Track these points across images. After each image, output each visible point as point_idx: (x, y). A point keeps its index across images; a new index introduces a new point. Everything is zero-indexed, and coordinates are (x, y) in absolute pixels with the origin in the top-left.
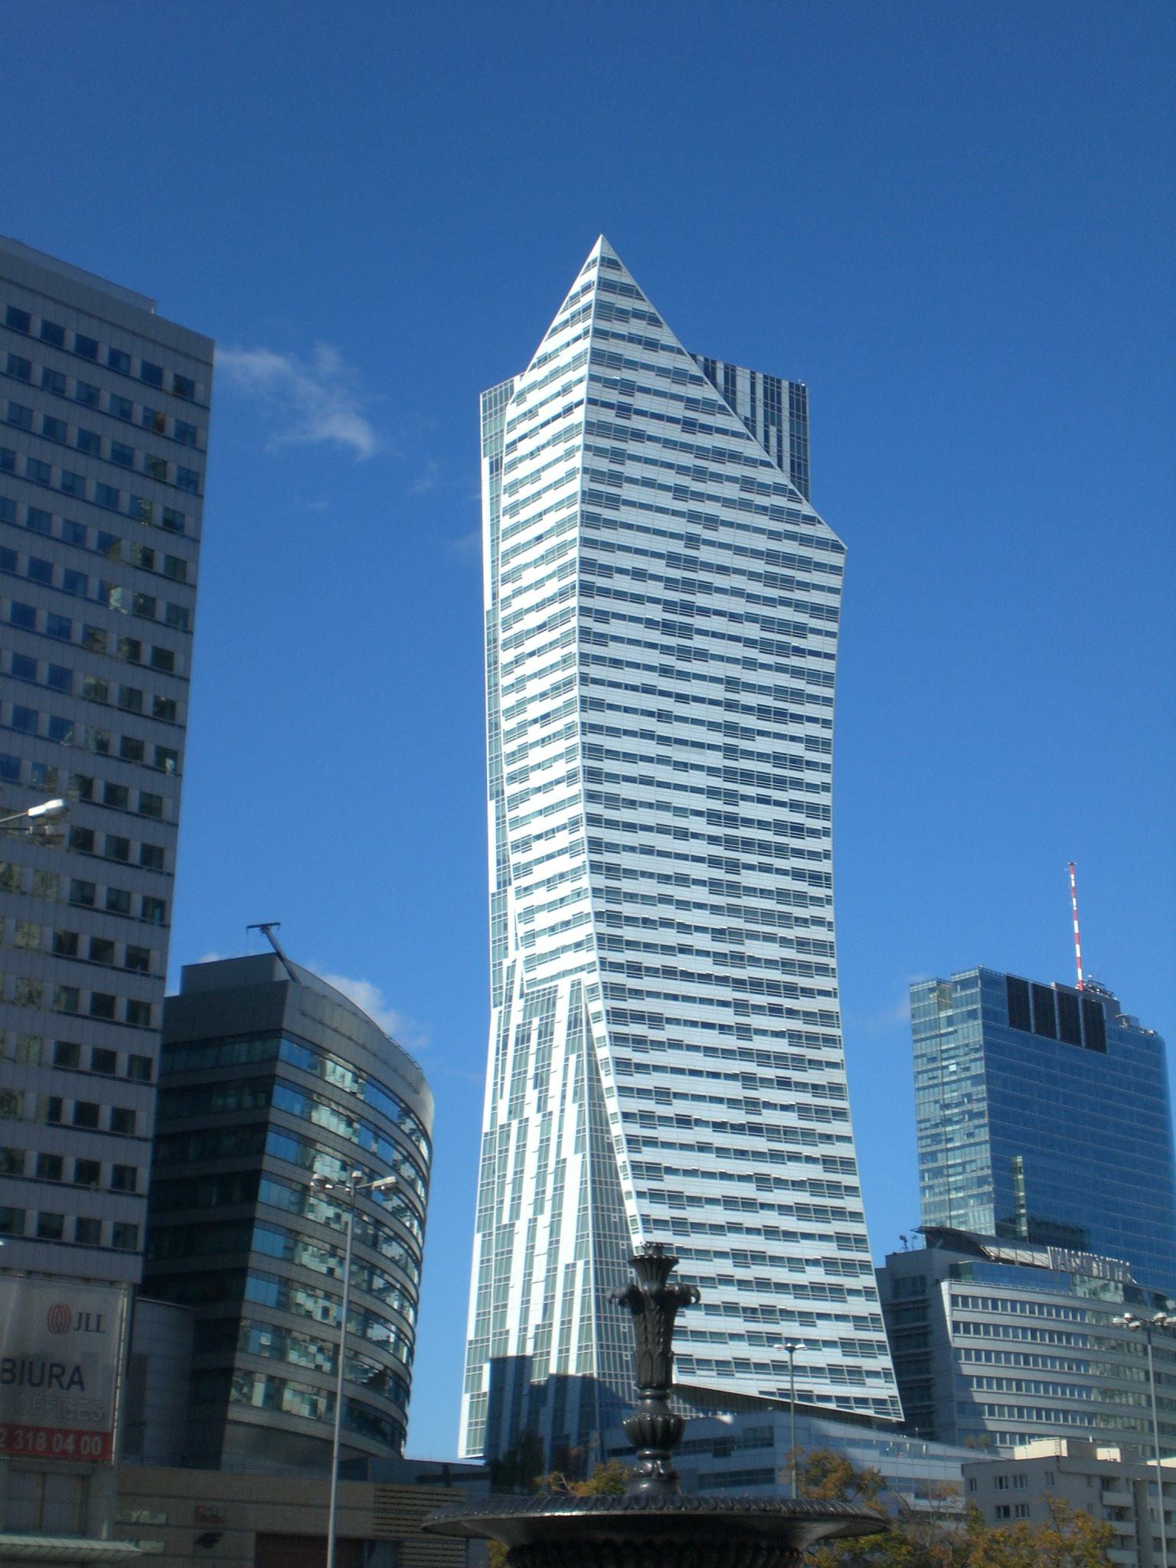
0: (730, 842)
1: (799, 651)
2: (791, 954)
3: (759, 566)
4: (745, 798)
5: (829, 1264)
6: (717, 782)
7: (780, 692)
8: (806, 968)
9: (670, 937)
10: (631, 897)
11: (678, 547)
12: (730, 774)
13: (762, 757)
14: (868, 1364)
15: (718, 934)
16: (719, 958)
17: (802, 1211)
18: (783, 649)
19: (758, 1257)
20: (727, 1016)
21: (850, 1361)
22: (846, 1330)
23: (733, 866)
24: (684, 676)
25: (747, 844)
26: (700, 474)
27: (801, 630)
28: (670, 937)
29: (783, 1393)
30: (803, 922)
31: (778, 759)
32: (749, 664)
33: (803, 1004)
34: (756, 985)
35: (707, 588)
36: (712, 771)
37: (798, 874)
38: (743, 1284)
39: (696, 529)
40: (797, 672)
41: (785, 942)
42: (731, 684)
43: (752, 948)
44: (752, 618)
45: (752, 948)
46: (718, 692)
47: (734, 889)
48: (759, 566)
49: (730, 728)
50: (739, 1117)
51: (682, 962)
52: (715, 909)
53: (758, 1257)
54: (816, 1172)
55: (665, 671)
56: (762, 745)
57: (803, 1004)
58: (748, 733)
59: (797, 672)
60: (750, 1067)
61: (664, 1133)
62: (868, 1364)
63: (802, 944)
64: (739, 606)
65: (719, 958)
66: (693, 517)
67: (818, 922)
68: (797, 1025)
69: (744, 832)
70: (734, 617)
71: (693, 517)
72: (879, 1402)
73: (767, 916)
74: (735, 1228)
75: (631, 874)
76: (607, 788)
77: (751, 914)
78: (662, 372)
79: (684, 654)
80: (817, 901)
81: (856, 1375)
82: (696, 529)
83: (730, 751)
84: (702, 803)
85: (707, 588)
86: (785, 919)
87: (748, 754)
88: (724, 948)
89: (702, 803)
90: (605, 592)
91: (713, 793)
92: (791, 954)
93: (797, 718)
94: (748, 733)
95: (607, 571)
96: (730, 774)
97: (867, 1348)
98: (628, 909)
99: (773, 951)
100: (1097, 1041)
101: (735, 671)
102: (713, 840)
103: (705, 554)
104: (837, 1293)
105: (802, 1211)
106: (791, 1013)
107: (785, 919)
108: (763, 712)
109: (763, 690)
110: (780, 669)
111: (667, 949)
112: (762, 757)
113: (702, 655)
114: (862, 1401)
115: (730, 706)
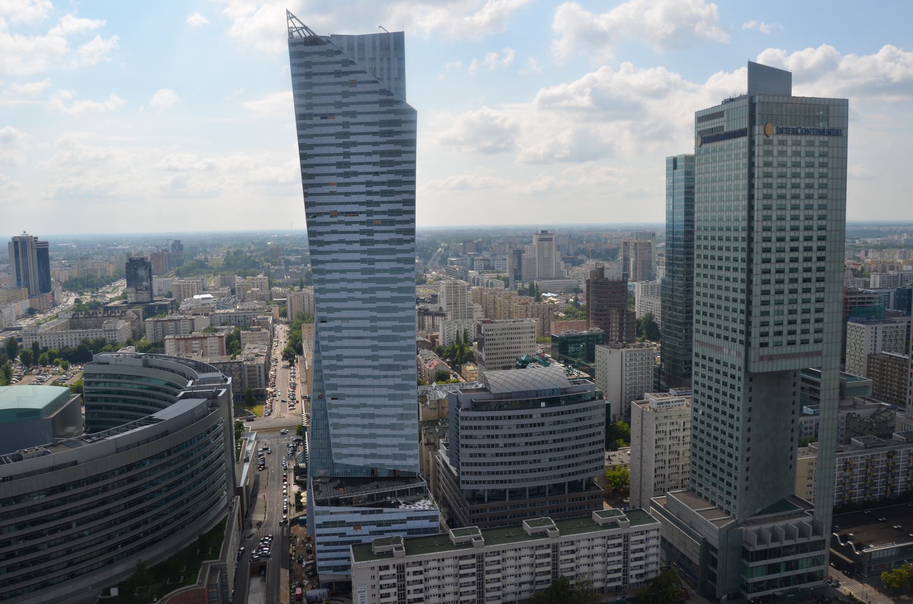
0: (369, 252)
1: (399, 163)
2: (395, 294)
3: (376, 129)
4: (376, 232)
6: (364, 227)
7: (390, 183)
9: (344, 295)
10: (330, 281)
11: (340, 129)
12: (369, 223)
13: (384, 213)
14: (410, 453)
15: (364, 291)
16: (364, 301)
18: (391, 163)
19: (372, 416)
20: (367, 324)
21: (402, 452)
22: (403, 441)
23: (372, 262)
24: (347, 184)
25: (378, 252)
26: (345, 94)
27: (398, 153)
28: (344, 295)
30: (401, 280)
31: (391, 212)
32: (377, 174)
33: (402, 314)
35: (354, 144)
36: (362, 223)
37: (399, 260)
38: (364, 426)
39: (347, 119)
40: (397, 173)
42: (369, 184)
43: (379, 295)
44: (375, 153)
45: (379, 295)
46: (363, 188)
48: (376, 129)
49: (369, 203)
50: (369, 363)
51: (351, 304)
52: (364, 281)
53: (372, 416)
54: (398, 381)
55: (339, 185)
56: (384, 208)
57: (402, 314)
58: (377, 204)
59: (397, 173)
60: (375, 343)
61: (339, 372)
62: (410, 453)
63: (400, 290)
64: (369, 149)
65: (364, 301)
66: (344, 114)
67: (407, 279)
69: (377, 246)
70: (368, 154)
71: (344, 114)
72: (410, 466)
73: (386, 280)
74: (364, 405)
75: (330, 272)
76: (319, 238)
77: (378, 281)
78: (321, 53)
79: (346, 175)
81: (404, 457)
82: (347, 119)
83: (369, 213)
84: (357, 237)
85: (354, 144)
87: (377, 213)
88: (367, 296)
89: (357, 237)
90: (312, 156)
91: (362, 232)
92: (395, 294)
93: (399, 193)
94: (377, 204)
95: (311, 147)
96: (369, 223)
98: (329, 286)
99: (387, 294)
101: (370, 178)
102: (362, 252)
103: (353, 129)
106: (394, 319)
108: (383, 193)
109: (382, 183)
110: (389, 172)
111: (344, 300)
112: (384, 213)
113: (355, 174)
115: (369, 193)
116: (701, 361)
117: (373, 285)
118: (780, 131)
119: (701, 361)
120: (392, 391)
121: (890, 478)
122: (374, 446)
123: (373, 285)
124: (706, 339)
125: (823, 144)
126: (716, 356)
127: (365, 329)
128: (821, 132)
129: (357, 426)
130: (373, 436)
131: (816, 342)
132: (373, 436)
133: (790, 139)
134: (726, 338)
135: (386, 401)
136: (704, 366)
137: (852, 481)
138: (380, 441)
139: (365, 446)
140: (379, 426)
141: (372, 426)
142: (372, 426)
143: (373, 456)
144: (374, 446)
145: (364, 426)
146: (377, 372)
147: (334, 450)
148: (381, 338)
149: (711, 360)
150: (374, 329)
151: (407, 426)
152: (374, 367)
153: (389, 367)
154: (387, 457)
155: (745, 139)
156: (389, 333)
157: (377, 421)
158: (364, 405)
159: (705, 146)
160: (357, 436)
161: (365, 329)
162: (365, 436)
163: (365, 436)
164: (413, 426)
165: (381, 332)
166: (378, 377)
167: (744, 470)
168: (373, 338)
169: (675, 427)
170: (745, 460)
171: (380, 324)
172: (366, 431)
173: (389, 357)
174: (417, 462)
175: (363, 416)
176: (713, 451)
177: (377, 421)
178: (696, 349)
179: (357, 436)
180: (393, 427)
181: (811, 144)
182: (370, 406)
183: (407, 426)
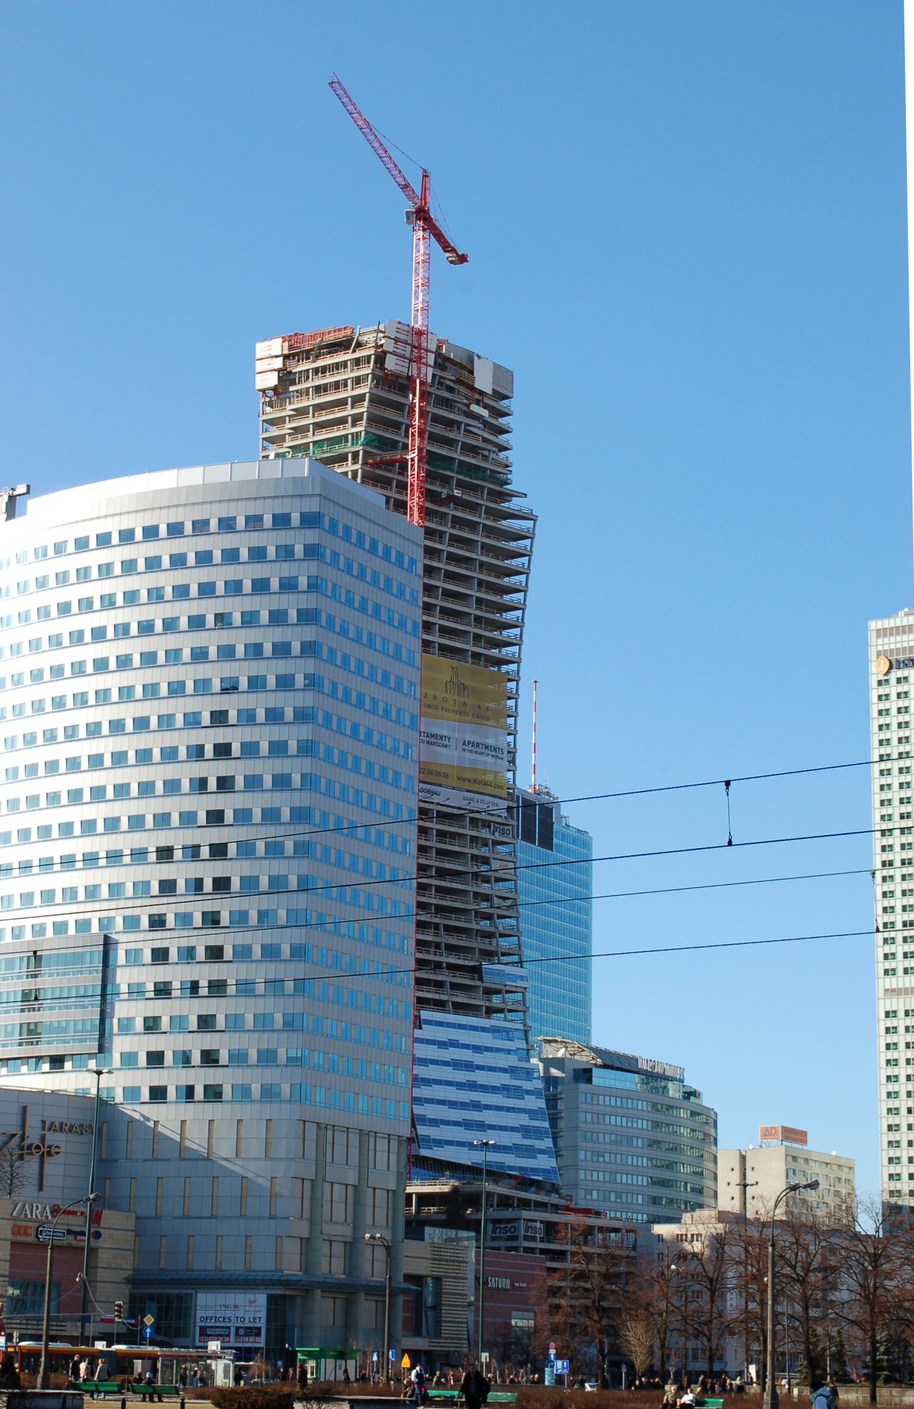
19: (470, 1066)
38: (459, 1085)
53: (470, 1066)
74: (454, 1044)
81: (531, 1152)
97: (538, 1133)
100: (547, 842)
104: (519, 1093)
114: (535, 1171)
122: (481, 1126)
129: (449, 1083)
130: (476, 1106)
132: (476, 1106)
138: (487, 1117)
139: (468, 1125)
140: (485, 1088)
141: (472, 1086)
142: (472, 1086)
144: (481, 1126)
145: (459, 1085)
154: (506, 1149)
158: (454, 1044)
160: (453, 1104)
162: (463, 1106)
163: (463, 1106)
175: (456, 1064)
177: (481, 1077)
179: (453, 1104)
182: (466, 1046)
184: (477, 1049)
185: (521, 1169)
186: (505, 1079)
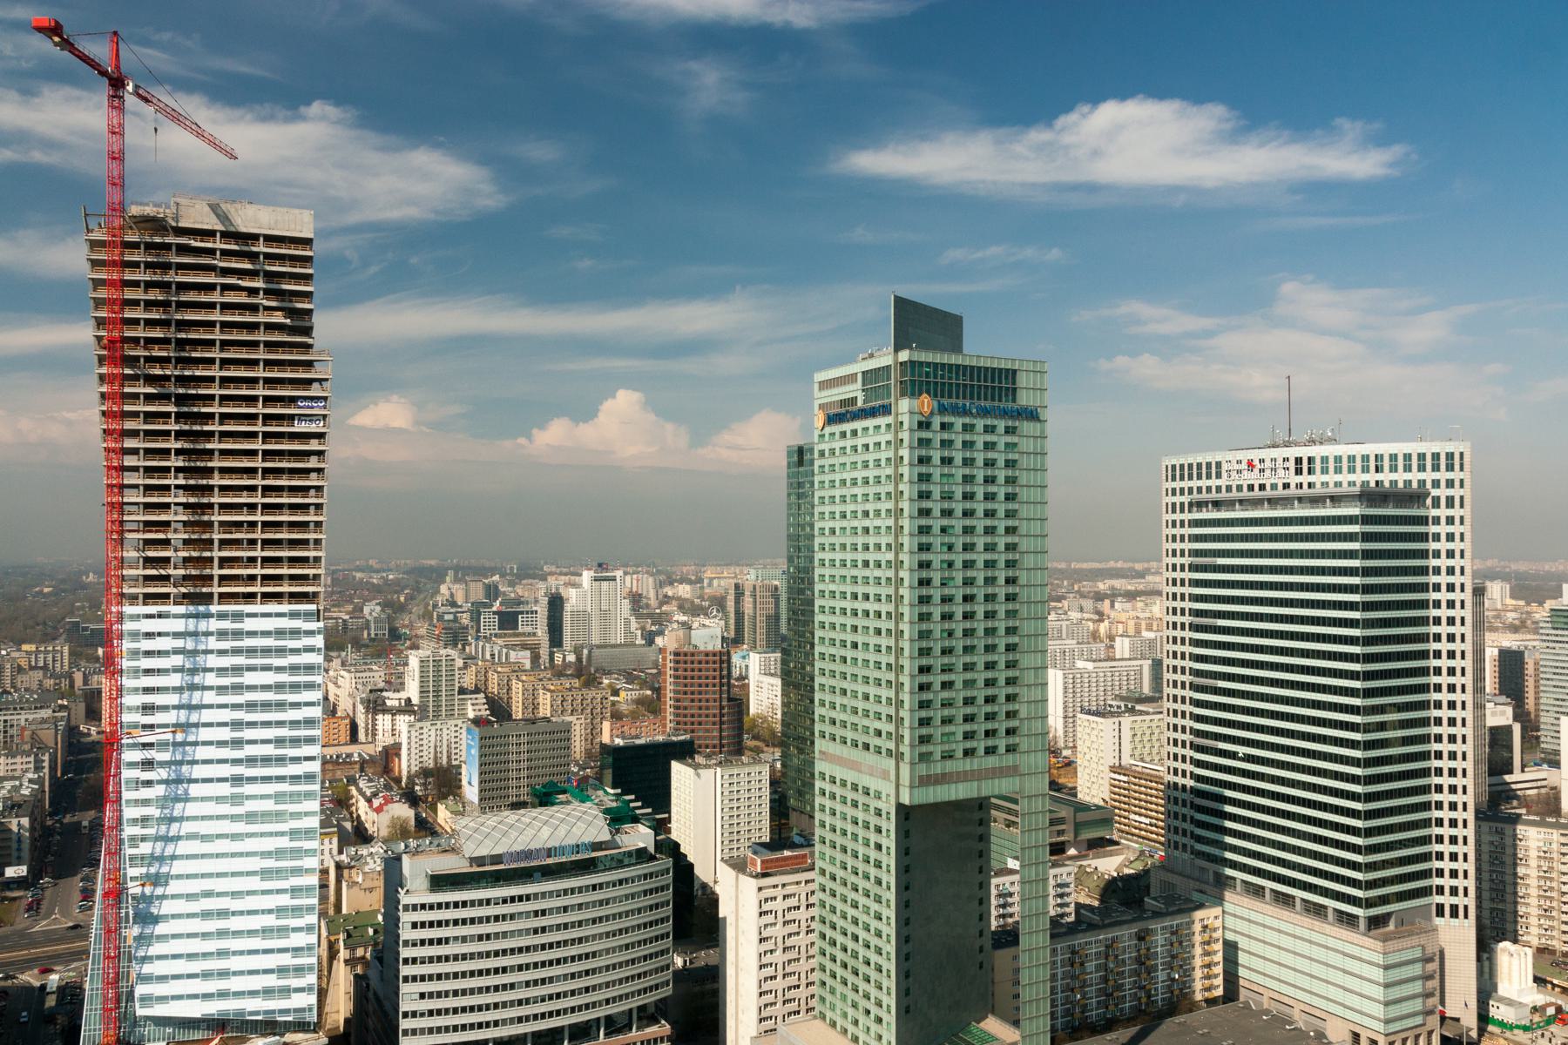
2: (284, 678)
5: (280, 911)
8: (295, 687)
14: (295, 983)
17: (265, 874)
19: (223, 914)
22: (286, 960)
29: (220, 1013)
34: (251, 706)
38: (205, 936)
41: (279, 669)
43: (249, 678)
45: (249, 678)
47: (238, 634)
50: (226, 809)
53: (223, 914)
54: (284, 843)
62: (295, 983)
63: (294, 669)
68: (284, 732)
72: (296, 1010)
73: (266, 651)
74: (208, 894)
77: (251, 651)
80: (310, 633)
81: (286, 992)
86: (281, 651)
92: (284, 678)
104: (283, 931)
105: (265, 874)
107: (281, 651)
114: (283, 1012)
116: (828, 787)
117: (240, 660)
118: (943, 410)
119: (828, 787)
120: (270, 863)
121: (1144, 976)
123: (240, 660)
124: (835, 749)
125: (1008, 431)
126: (851, 776)
127: (221, 744)
128: (1005, 414)
130: (222, 954)
131: (1010, 749)
132: (222, 954)
133: (958, 422)
134: (867, 747)
135: (255, 883)
136: (833, 797)
137: (1084, 985)
140: (237, 934)
141: (222, 934)
142: (222, 934)
143: (223, 995)
144: (224, 974)
145: (205, 936)
146: (240, 827)
147: (140, 990)
148: (251, 761)
149: (844, 783)
150: (237, 743)
151: (295, 930)
152: (234, 818)
153: (266, 816)
155: (889, 419)
156: (269, 750)
157: (235, 923)
159: (828, 430)
161: (222, 744)
164: (309, 929)
165: (250, 750)
166: (235, 837)
167: (902, 977)
168: (236, 762)
169: (793, 902)
170: (903, 957)
171: (248, 734)
172: (211, 946)
173: (263, 797)
174: (312, 999)
175: (206, 915)
176: (850, 945)
177: (235, 923)
178: (820, 766)
179: (191, 956)
180: (266, 932)
181: (989, 429)
183: (295, 930)
184: (235, 895)
185: (266, 1012)
186: (270, 921)
